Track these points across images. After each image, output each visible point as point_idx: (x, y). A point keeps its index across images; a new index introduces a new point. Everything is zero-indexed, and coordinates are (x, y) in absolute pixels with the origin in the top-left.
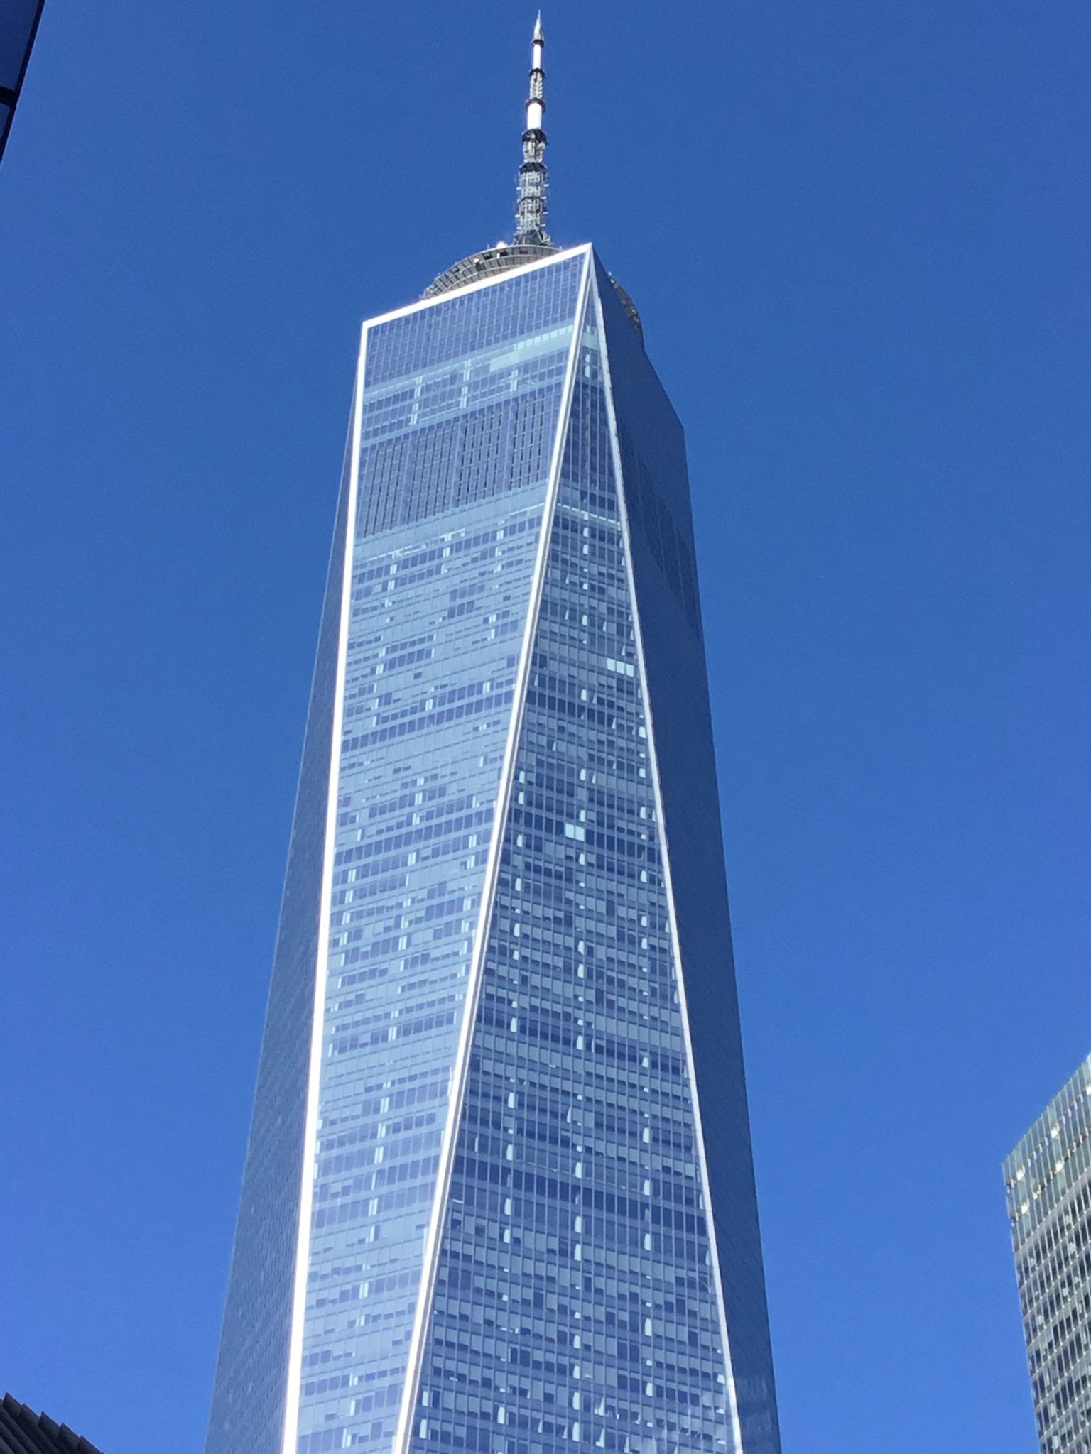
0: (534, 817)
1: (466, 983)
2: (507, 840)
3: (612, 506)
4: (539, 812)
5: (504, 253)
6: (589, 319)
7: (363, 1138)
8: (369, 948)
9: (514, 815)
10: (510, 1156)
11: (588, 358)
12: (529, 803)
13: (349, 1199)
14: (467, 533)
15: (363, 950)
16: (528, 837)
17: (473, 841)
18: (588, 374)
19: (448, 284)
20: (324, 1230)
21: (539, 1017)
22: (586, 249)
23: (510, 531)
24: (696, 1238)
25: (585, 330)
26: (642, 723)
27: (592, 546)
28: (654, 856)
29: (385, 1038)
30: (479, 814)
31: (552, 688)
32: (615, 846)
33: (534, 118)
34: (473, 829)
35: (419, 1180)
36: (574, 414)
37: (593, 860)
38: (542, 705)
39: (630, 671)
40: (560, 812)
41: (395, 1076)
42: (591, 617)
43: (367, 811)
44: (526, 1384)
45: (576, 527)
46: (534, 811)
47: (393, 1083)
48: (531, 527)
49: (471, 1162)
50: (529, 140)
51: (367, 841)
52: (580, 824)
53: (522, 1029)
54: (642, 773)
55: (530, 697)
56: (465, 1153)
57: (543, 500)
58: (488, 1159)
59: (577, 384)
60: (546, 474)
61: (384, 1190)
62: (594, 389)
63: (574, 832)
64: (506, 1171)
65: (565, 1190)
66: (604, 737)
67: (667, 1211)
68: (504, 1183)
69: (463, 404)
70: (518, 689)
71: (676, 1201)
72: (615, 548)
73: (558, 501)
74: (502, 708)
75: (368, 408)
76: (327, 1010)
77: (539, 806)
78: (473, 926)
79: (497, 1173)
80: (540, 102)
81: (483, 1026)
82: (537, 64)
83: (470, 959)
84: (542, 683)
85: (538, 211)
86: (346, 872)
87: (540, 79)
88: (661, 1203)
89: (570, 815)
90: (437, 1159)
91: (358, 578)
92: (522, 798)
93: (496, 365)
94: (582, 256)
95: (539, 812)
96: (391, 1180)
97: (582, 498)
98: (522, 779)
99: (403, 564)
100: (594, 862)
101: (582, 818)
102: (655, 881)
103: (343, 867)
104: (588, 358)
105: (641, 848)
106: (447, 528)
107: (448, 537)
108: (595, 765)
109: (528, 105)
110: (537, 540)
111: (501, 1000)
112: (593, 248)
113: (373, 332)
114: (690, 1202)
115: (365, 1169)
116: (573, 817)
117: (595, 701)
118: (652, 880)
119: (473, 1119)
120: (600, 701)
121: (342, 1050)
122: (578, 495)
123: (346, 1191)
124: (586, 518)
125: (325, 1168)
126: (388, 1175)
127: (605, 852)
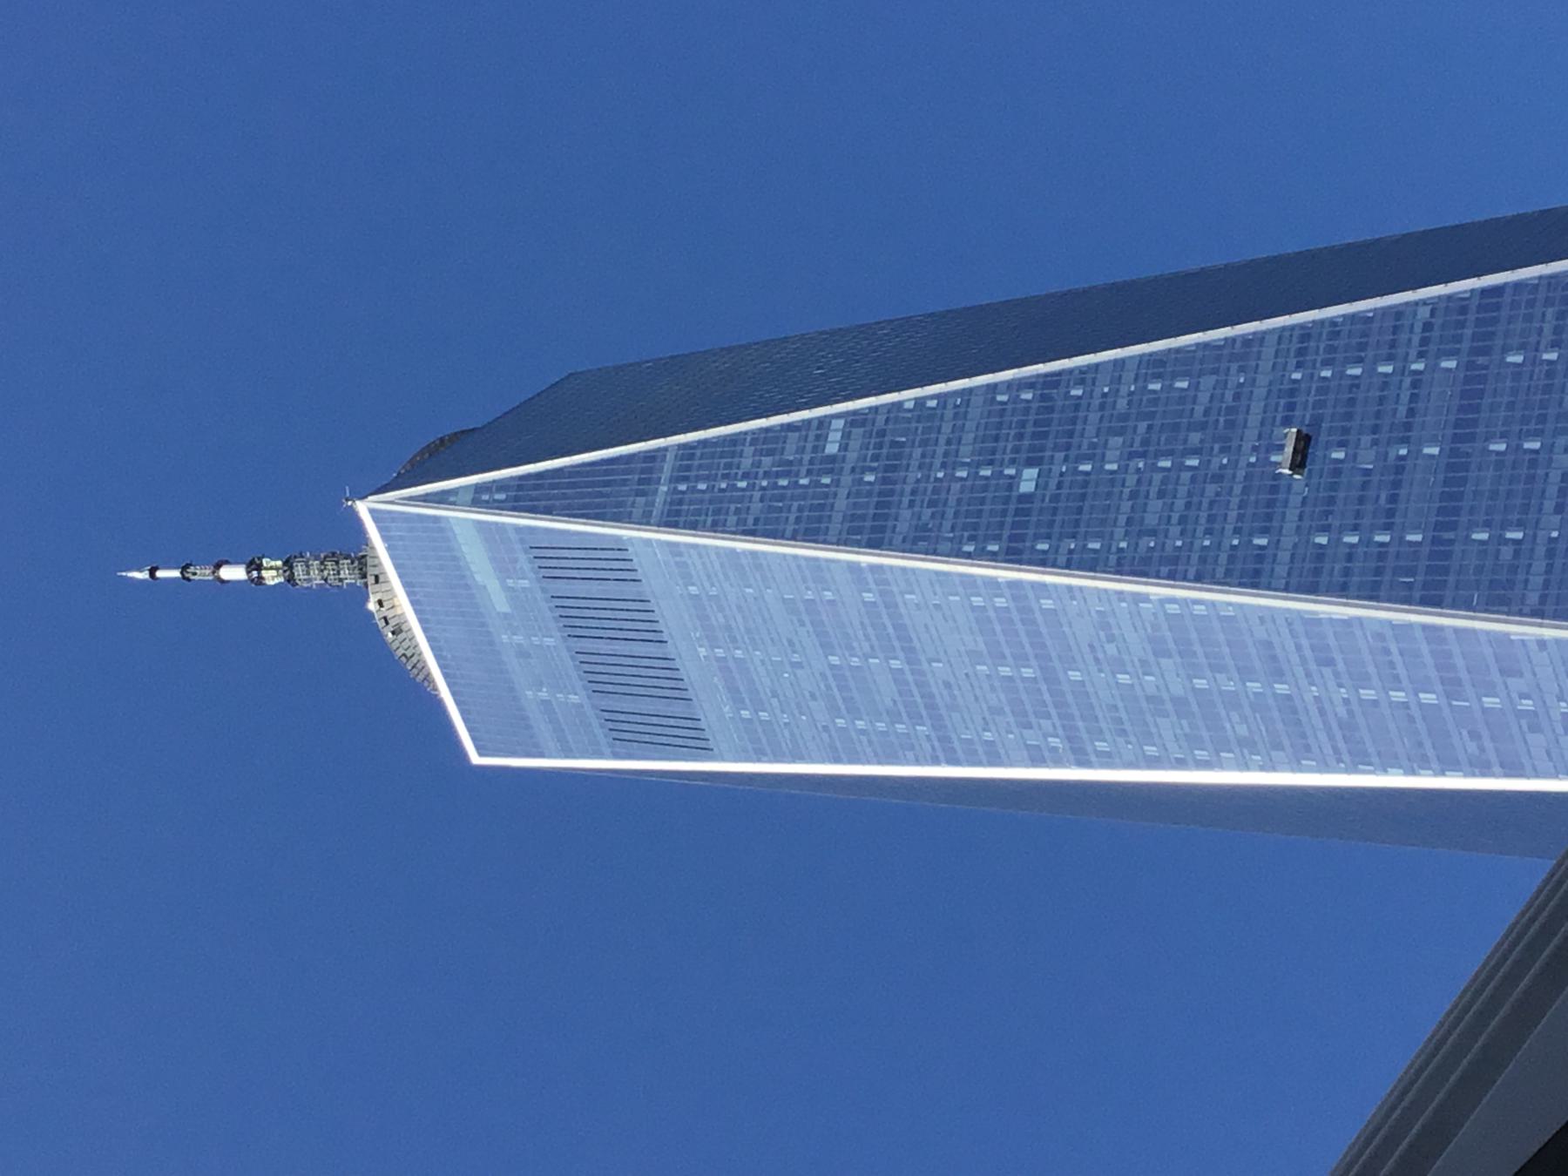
0: (1015, 533)
1: (1213, 604)
2: (1043, 563)
3: (651, 457)
4: (1007, 526)
5: (380, 603)
6: (441, 499)
7: (1411, 719)
8: (1184, 722)
9: (1014, 555)
10: (1418, 538)
11: (485, 497)
13: (1485, 734)
14: (696, 629)
15: (1187, 730)
16: (1037, 537)
17: (1047, 604)
18: (501, 496)
19: (421, 666)
20: (1525, 760)
21: (1250, 511)
22: (362, 508)
23: (688, 580)
24: (1507, 298)
25: (454, 503)
26: (899, 405)
27: (698, 479)
29: (1289, 697)
30: (1015, 598)
31: (863, 518)
33: (234, 573)
34: (1035, 607)
35: (1456, 649)
36: (548, 511)
37: (1060, 455)
38: (882, 529)
39: (840, 424)
40: (1007, 500)
41: (1332, 684)
42: (778, 475)
43: (1026, 732)
46: (1006, 533)
47: (1340, 686)
48: (680, 554)
49: (1425, 586)
50: (260, 578)
51: (1060, 732)
52: (1019, 474)
53: (1264, 531)
55: (875, 544)
56: (1417, 595)
57: (648, 542)
58: (1423, 564)
59: (514, 509)
60: (618, 539)
61: (1469, 690)
62: (520, 488)
63: (1028, 480)
64: (1436, 541)
65: (1456, 466)
66: (918, 452)
67: (1474, 337)
68: (1451, 542)
69: (549, 641)
70: (866, 559)
71: (1463, 327)
72: (698, 452)
73: (648, 524)
74: (889, 576)
75: (568, 754)
76: (1262, 768)
77: (1001, 525)
78: (1145, 598)
79: (1440, 551)
80: (218, 566)
81: (1264, 580)
82: (176, 574)
83: (1185, 600)
84: (859, 531)
85: (337, 563)
86: (1099, 754)
87: (192, 569)
88: (1465, 345)
89: (1010, 487)
90: (1425, 627)
91: (759, 756)
92: (994, 548)
93: (501, 604)
94: (372, 511)
95: (1007, 526)
96: (1459, 682)
98: (969, 548)
99: (738, 702)
100: (1062, 454)
101: (1011, 471)
102: (1083, 376)
103: (1093, 758)
104: (485, 497)
105: (1043, 398)
106: (693, 656)
107: (702, 651)
108: (951, 459)
109: (223, 582)
110: (695, 546)
111: (1231, 559)
112: (363, 498)
113: (482, 751)
114: (1463, 310)
115: (1446, 712)
116: (1013, 481)
117: (875, 464)
118: (1082, 382)
120: (876, 458)
121: (1308, 748)
122: (641, 500)
123: (1475, 735)
124: (665, 489)
125: (1447, 765)
126: (1452, 688)
127: (1050, 443)
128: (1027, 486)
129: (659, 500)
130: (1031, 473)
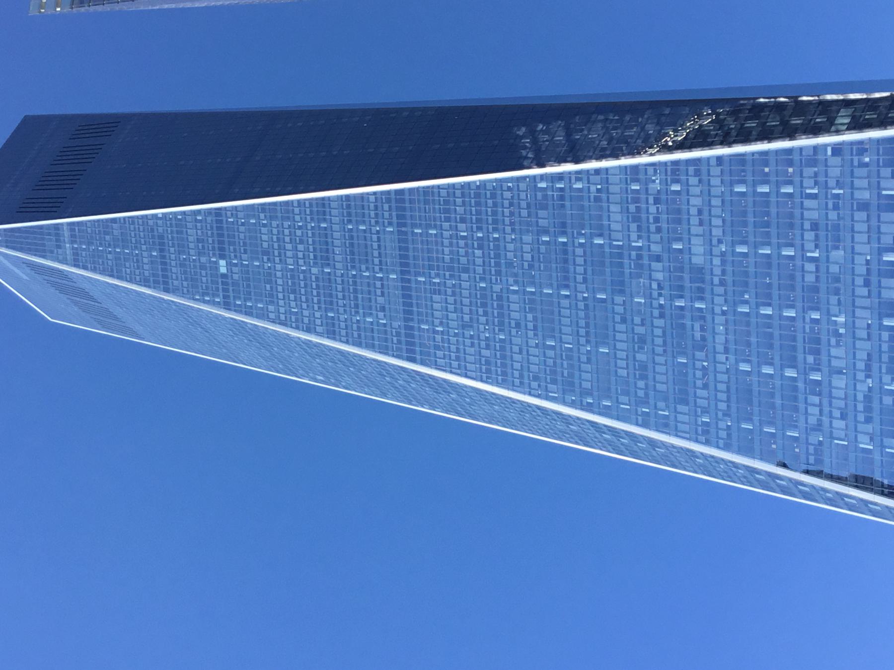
3: (57, 227)
9: (227, 306)
12: (218, 296)
28: (218, 212)
32: (221, 235)
44: (513, 323)
45: (76, 253)
54: (180, 217)
93: (25, 277)
97: (59, 247)
119: (387, 348)
122: (60, 251)
128: (223, 270)
129: (68, 252)
130: (222, 263)
